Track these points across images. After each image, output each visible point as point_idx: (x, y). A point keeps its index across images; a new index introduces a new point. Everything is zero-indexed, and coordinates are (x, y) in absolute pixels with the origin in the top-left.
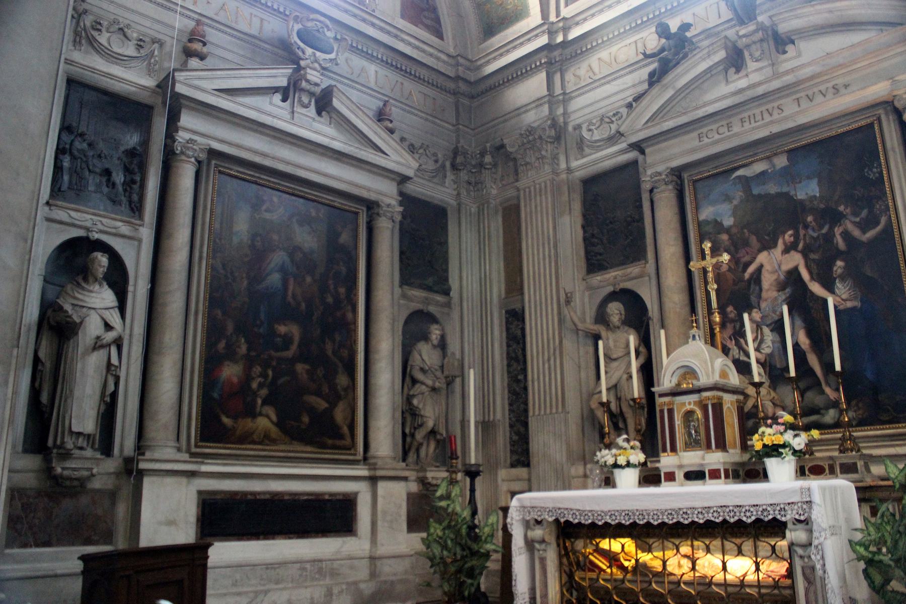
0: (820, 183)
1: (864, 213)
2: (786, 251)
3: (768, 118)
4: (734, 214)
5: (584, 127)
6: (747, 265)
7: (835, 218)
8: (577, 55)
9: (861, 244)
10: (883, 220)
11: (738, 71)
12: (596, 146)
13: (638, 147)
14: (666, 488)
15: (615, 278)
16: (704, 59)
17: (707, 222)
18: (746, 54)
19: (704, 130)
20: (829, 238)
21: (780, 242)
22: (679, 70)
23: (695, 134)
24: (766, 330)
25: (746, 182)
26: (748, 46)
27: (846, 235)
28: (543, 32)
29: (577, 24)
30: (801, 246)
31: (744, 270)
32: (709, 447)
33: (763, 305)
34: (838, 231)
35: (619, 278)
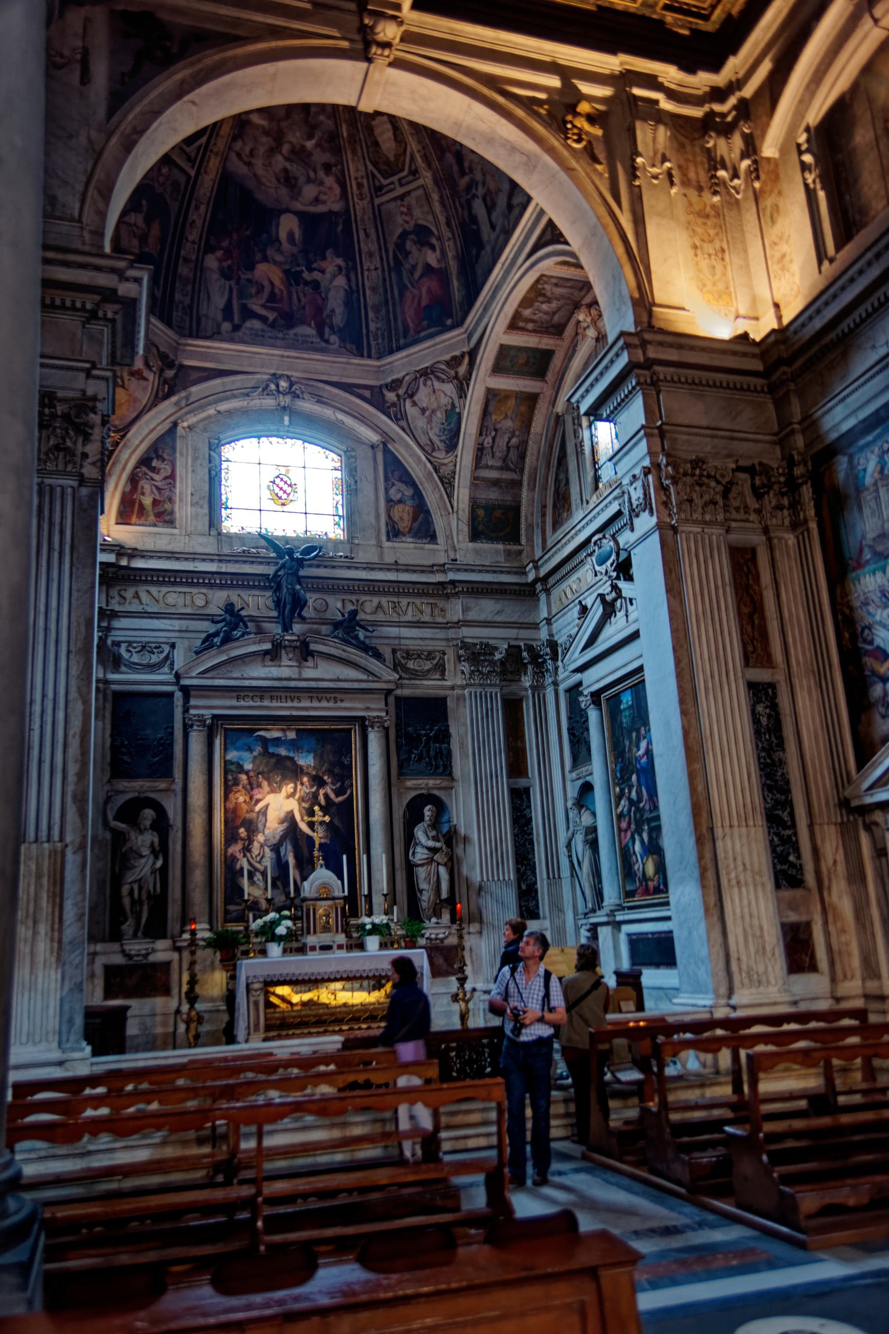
0: (314, 758)
1: (339, 785)
2: (288, 796)
3: (290, 704)
4: (253, 761)
5: (123, 646)
6: (258, 801)
7: (321, 783)
8: (129, 579)
9: (334, 803)
10: (349, 792)
11: (272, 660)
12: (134, 667)
13: (186, 691)
14: (311, 956)
15: (142, 787)
16: (255, 643)
17: (232, 763)
18: (283, 652)
19: (242, 694)
20: (315, 796)
21: (284, 790)
22: (235, 644)
23: (235, 694)
24: (267, 850)
25: (265, 742)
26: (285, 647)
27: (326, 796)
28: (113, 551)
29: (143, 557)
30: (297, 796)
31: (256, 804)
32: (337, 931)
33: (267, 832)
34: (322, 792)
35: (145, 788)
